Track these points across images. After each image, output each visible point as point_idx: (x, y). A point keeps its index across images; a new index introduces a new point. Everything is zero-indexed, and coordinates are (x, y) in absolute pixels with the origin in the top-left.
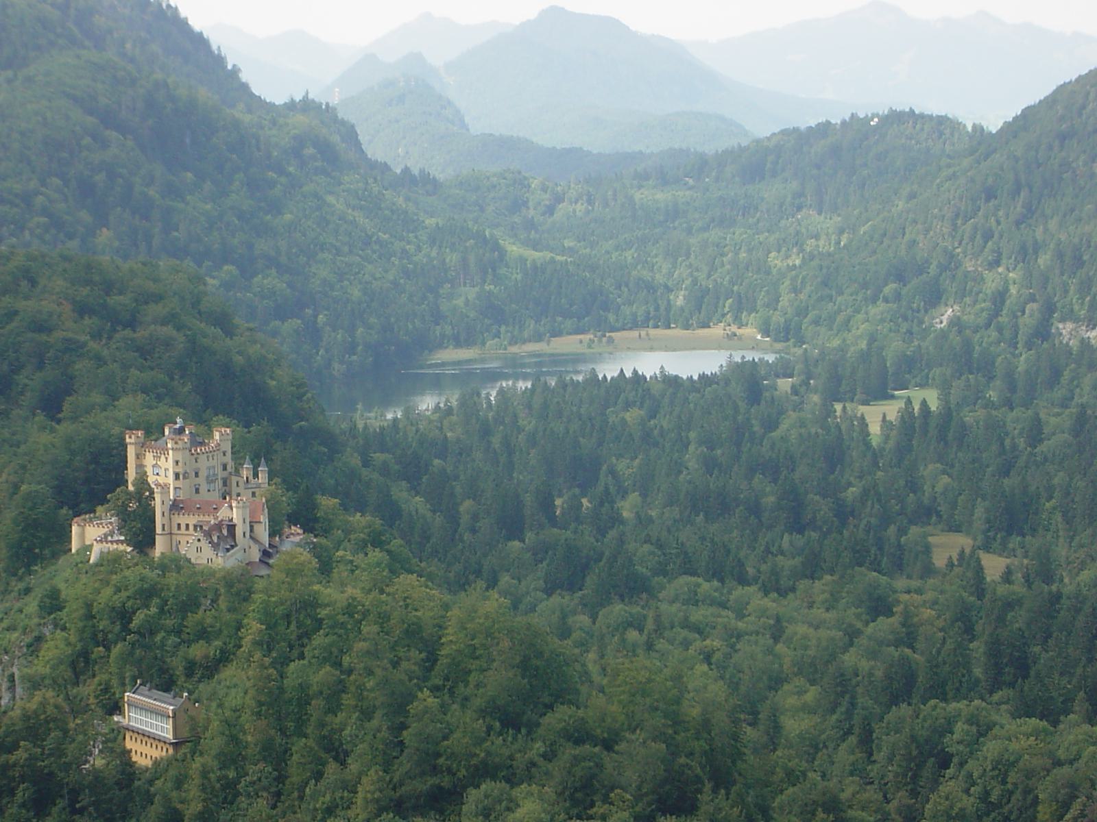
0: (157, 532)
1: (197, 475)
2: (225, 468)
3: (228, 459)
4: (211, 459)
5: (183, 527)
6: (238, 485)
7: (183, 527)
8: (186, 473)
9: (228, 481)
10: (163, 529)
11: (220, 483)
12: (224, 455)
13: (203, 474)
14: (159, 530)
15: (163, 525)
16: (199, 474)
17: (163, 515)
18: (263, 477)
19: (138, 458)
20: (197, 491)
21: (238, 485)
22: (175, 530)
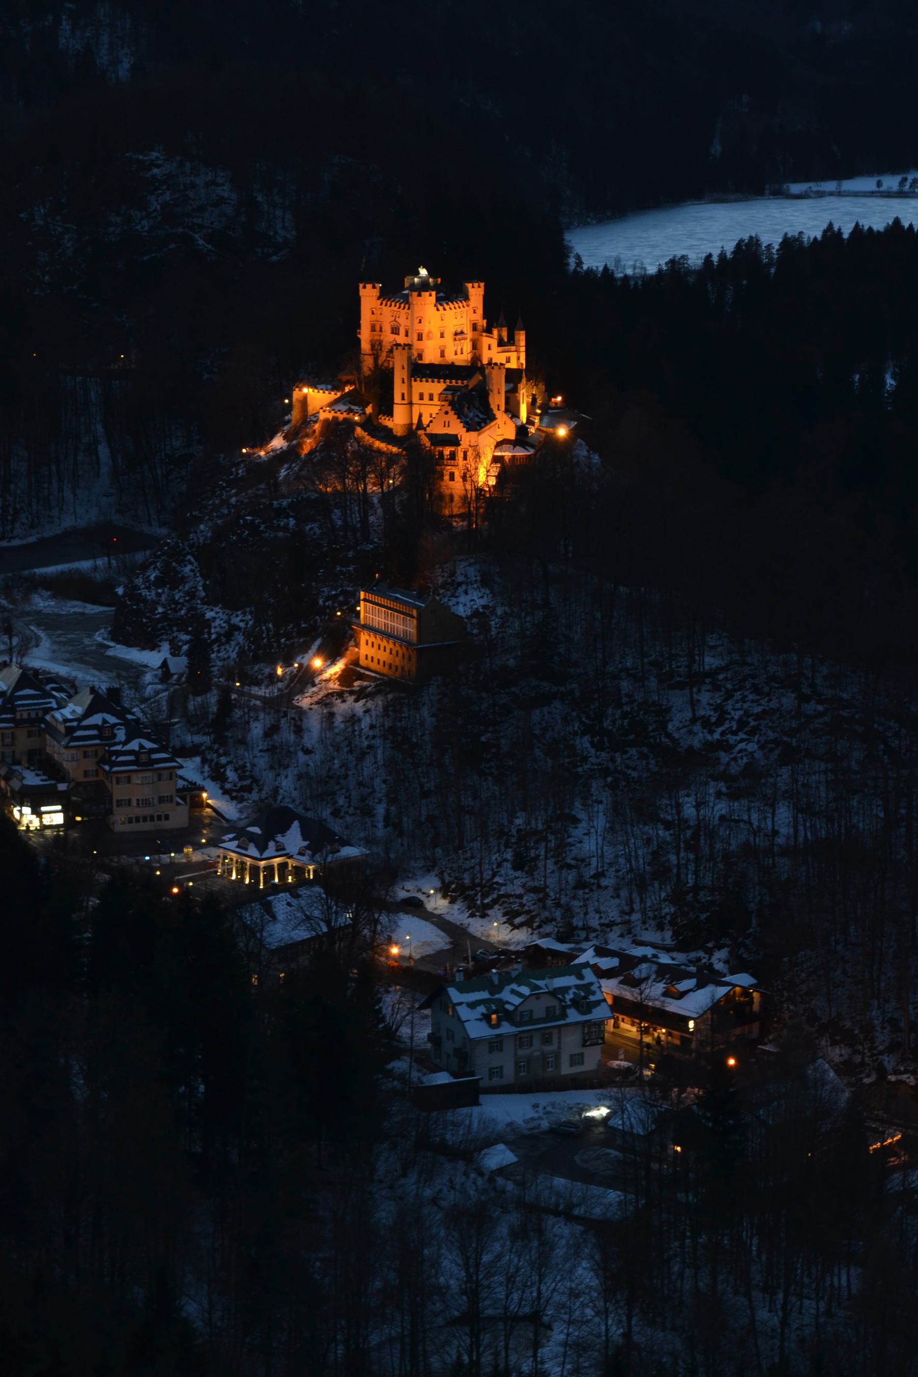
0: (395, 402)
1: (442, 336)
2: (474, 327)
3: (479, 317)
4: (459, 317)
5: (426, 397)
6: (489, 349)
7: (426, 397)
8: (430, 332)
9: (478, 343)
10: (403, 399)
11: (467, 346)
12: (474, 312)
13: (449, 336)
14: (397, 398)
15: (403, 395)
16: (446, 335)
17: (403, 382)
18: (521, 337)
19: (373, 313)
20: (442, 354)
21: (489, 349)
22: (415, 399)
